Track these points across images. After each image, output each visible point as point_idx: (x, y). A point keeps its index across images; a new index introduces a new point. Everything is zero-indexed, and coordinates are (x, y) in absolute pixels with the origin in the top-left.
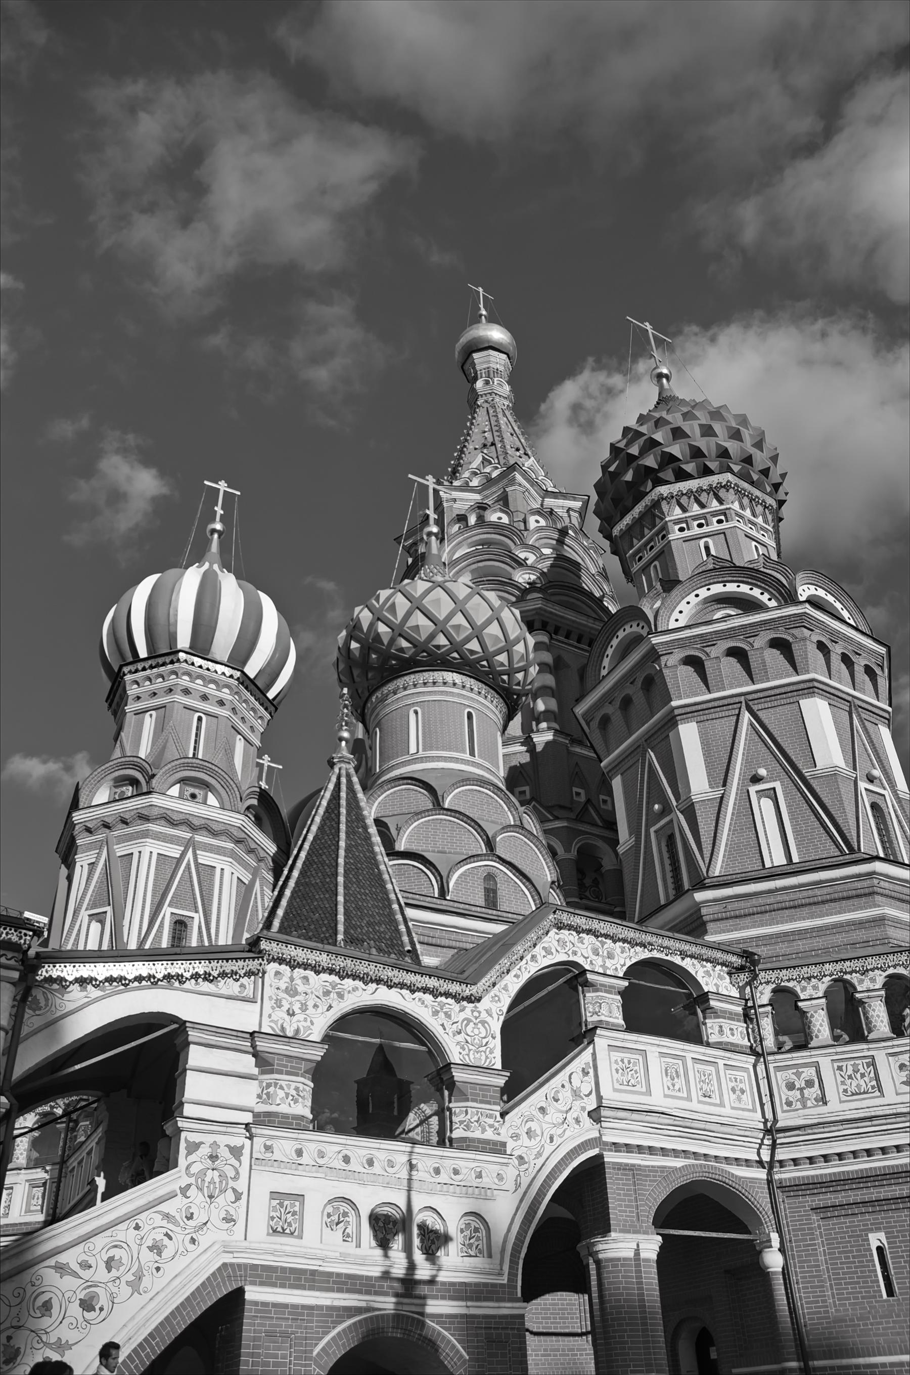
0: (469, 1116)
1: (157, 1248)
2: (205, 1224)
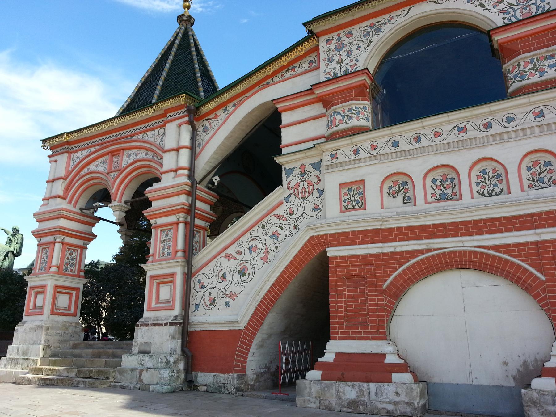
0: (522, 68)
1: (275, 236)
2: (302, 215)
